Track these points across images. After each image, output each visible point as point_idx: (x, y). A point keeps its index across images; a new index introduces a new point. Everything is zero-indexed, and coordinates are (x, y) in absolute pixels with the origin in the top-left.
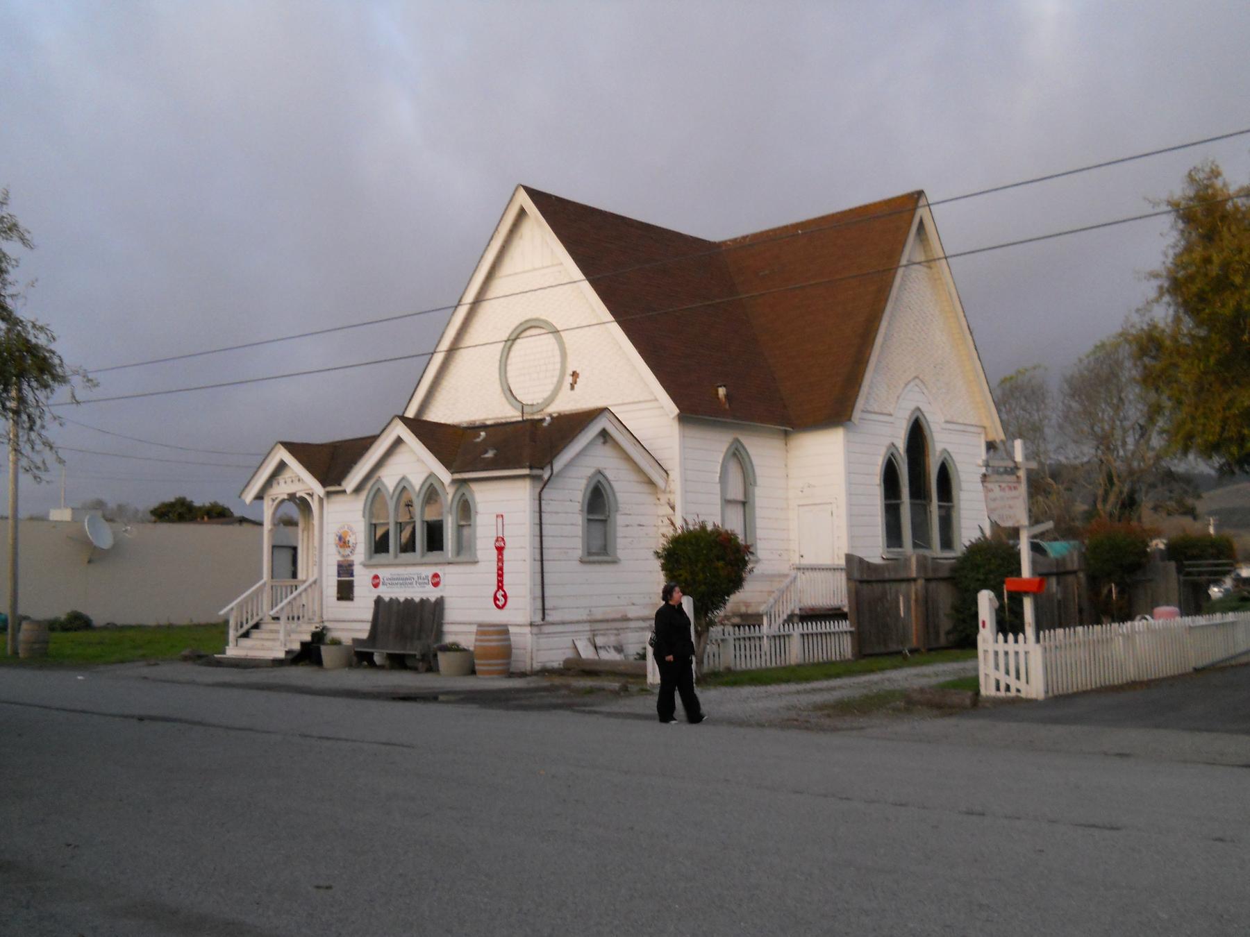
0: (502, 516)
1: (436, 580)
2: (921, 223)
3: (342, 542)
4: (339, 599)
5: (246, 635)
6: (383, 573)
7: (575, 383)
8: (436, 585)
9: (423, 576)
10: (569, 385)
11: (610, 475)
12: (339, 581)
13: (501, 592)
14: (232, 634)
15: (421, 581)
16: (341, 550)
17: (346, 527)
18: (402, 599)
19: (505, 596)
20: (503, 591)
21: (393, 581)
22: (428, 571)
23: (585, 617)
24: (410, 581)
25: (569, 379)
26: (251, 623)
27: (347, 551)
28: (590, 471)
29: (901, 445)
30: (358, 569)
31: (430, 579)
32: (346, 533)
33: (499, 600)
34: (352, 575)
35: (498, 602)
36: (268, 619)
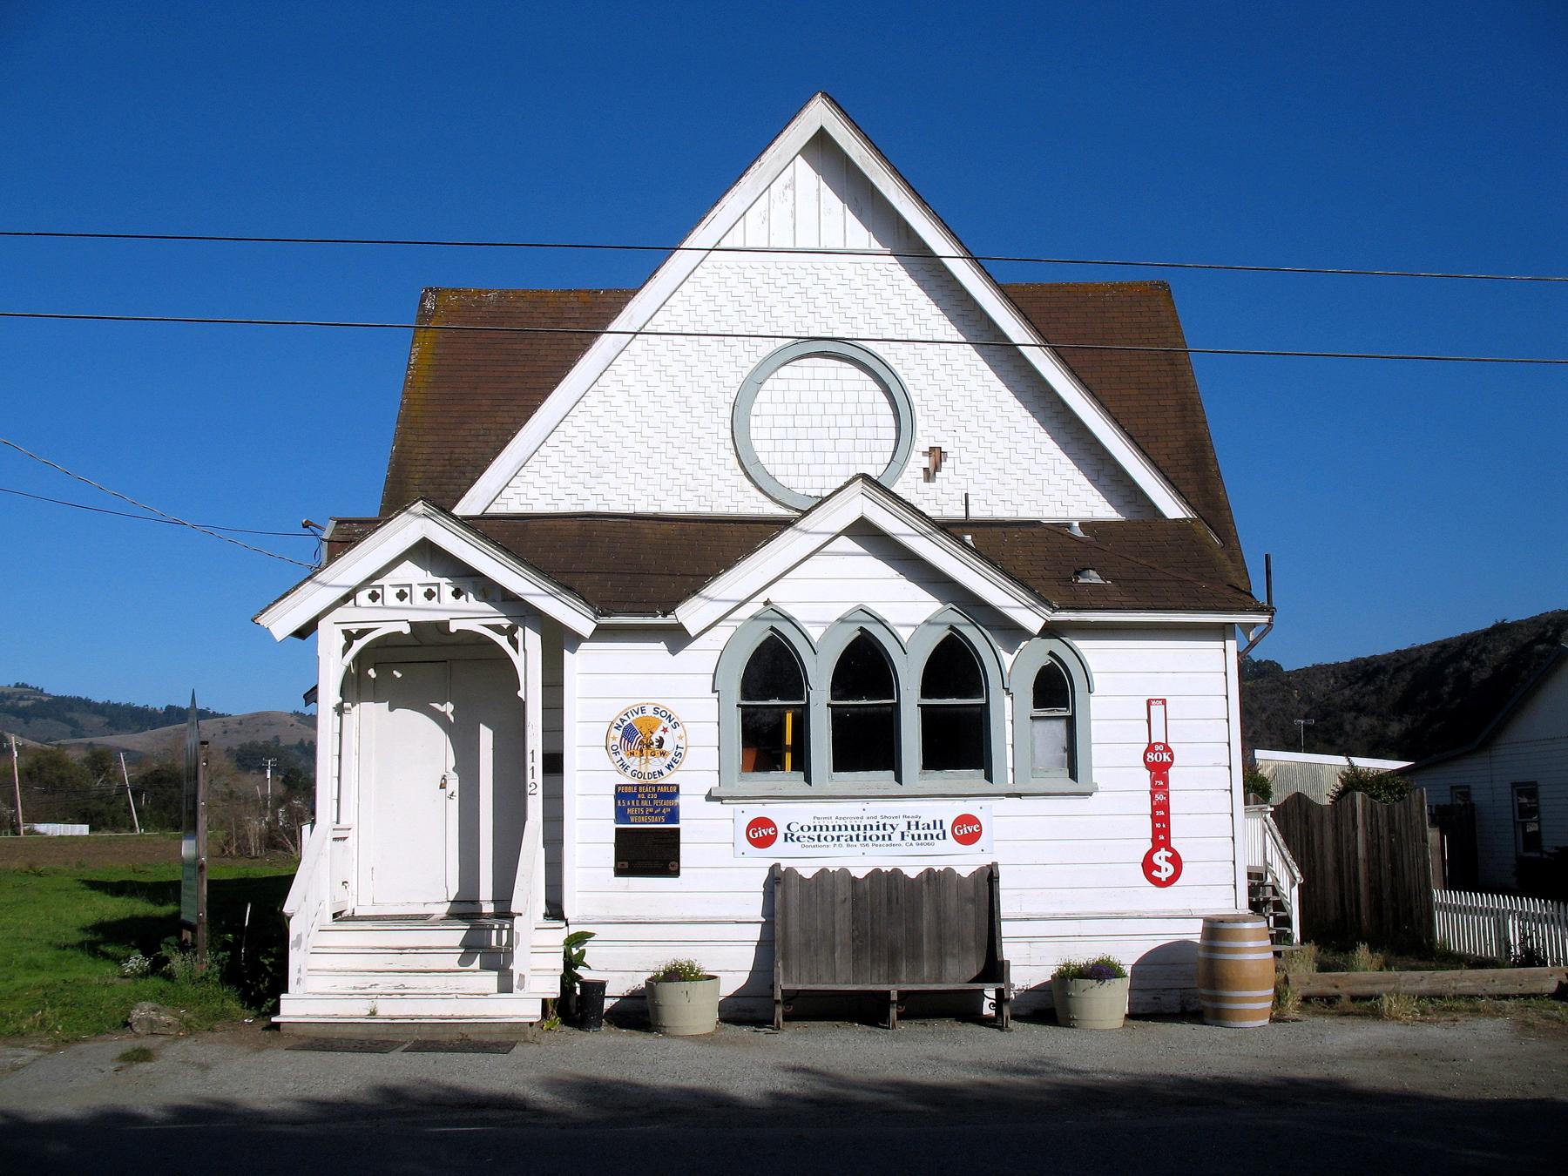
0: (1164, 702)
4: (619, 872)
6: (781, 814)
8: (969, 839)
10: (921, 474)
12: (617, 830)
13: (1163, 853)
15: (918, 832)
17: (649, 712)
19: (1176, 860)
20: (1169, 849)
21: (819, 833)
22: (949, 811)
24: (881, 833)
27: (656, 764)
34: (673, 816)
35: (1155, 873)
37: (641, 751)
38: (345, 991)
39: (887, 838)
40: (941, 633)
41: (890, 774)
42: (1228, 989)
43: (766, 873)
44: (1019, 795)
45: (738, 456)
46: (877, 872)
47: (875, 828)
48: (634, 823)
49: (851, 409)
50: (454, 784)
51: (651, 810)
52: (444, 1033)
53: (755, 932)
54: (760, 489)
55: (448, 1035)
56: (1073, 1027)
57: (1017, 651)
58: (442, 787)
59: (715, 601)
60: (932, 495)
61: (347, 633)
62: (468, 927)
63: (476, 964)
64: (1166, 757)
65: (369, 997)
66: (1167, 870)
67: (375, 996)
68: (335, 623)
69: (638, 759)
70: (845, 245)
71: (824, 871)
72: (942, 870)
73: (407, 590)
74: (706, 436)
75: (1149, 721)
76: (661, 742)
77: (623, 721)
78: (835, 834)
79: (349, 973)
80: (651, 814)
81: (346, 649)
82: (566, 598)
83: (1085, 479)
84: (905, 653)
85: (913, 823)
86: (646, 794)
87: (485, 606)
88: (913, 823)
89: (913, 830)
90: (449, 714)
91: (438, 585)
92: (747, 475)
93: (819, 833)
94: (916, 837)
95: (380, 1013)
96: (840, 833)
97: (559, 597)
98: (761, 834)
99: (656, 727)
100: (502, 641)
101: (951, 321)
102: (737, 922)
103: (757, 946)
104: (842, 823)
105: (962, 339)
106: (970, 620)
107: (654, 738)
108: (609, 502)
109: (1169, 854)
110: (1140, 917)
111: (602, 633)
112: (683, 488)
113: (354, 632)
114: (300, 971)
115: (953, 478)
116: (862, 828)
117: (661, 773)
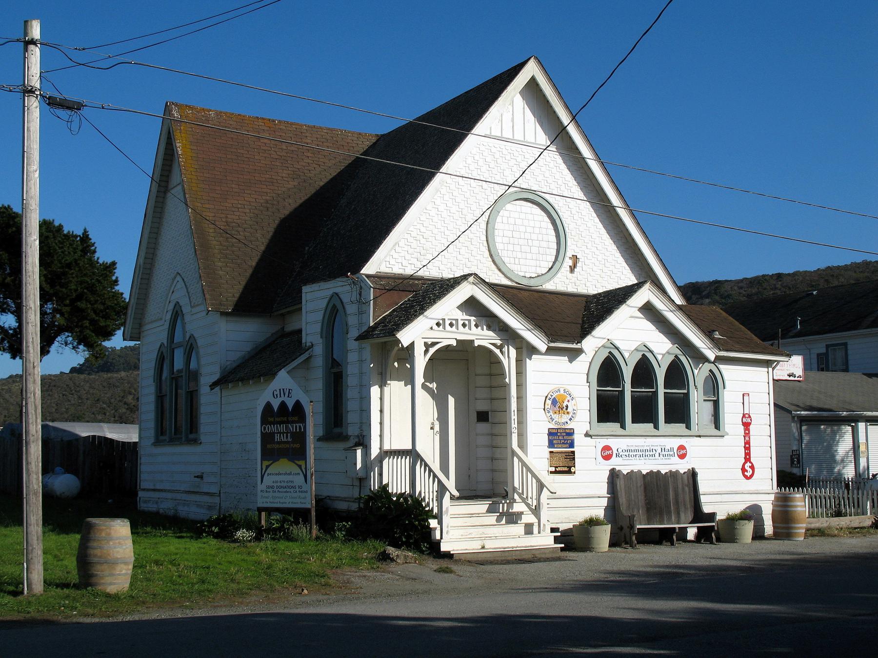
0: (749, 394)
1: (683, 452)
8: (682, 457)
9: (668, 447)
10: (568, 269)
13: (748, 464)
15: (665, 453)
17: (562, 392)
19: (752, 467)
20: (751, 462)
21: (629, 453)
22: (675, 443)
24: (651, 453)
25: (568, 262)
27: (565, 418)
31: (675, 451)
33: (747, 471)
34: (572, 445)
35: (746, 473)
37: (559, 411)
38: (458, 537)
39: (653, 455)
40: (672, 358)
41: (651, 425)
42: (795, 523)
43: (608, 473)
44: (700, 436)
45: (489, 250)
46: (651, 472)
47: (649, 451)
48: (556, 448)
49: (537, 230)
50: (437, 428)
51: (563, 441)
52: (525, 555)
53: (604, 502)
54: (500, 270)
55: (527, 556)
56: (737, 542)
57: (698, 368)
58: (432, 428)
59: (596, 338)
60: (574, 280)
61: (426, 344)
62: (491, 502)
63: (504, 522)
64: (749, 421)
65: (482, 539)
66: (748, 474)
67: (484, 538)
68: (423, 338)
69: (558, 415)
70: (536, 141)
71: (632, 471)
72: (663, 472)
73: (454, 322)
74: (474, 238)
75: (743, 403)
76: (567, 406)
77: (552, 396)
78: (635, 453)
79: (460, 528)
80: (563, 443)
81: (426, 352)
82: (537, 332)
83: (635, 278)
84: (627, 365)
85: (663, 449)
86: (561, 433)
87: (491, 333)
88: (663, 449)
89: (663, 453)
90: (434, 389)
91: (469, 321)
92: (494, 261)
93: (629, 453)
94: (664, 456)
95: (486, 547)
96: (636, 453)
97: (533, 332)
98: (607, 453)
99: (565, 399)
100: (497, 351)
101: (581, 189)
102: (599, 497)
103: (605, 509)
104: (637, 448)
105: (585, 199)
106: (682, 352)
107: (564, 405)
108: (430, 270)
109: (750, 465)
110: (743, 493)
111: (550, 351)
112: (464, 266)
113: (430, 343)
114: (448, 527)
115: (582, 272)
116: (644, 451)
117: (567, 423)
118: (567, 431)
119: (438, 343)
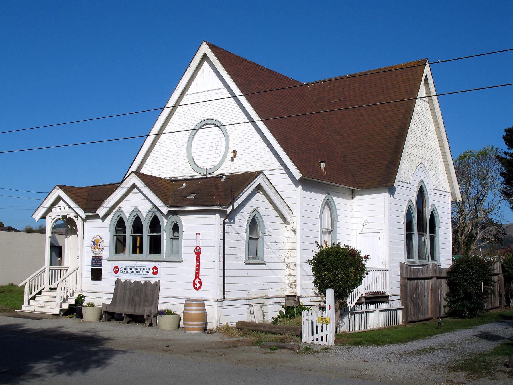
0: (200, 234)
1: (155, 271)
2: (426, 77)
3: (96, 244)
4: (92, 279)
5: (33, 298)
6: (121, 265)
7: (235, 157)
8: (155, 273)
9: (147, 268)
11: (261, 211)
12: (92, 268)
13: (198, 280)
14: (26, 298)
15: (145, 271)
16: (95, 250)
18: (132, 282)
19: (200, 282)
20: (199, 279)
21: (127, 270)
22: (151, 265)
23: (246, 296)
24: (138, 271)
26: (37, 291)
27: (99, 251)
28: (251, 210)
29: (414, 201)
30: (104, 262)
31: (151, 270)
32: (98, 240)
33: (196, 285)
34: (101, 265)
35: (195, 286)
36: (47, 289)
64: (200, 251)
76: (99, 245)
78: (129, 271)
80: (97, 264)
85: (144, 268)
86: (97, 259)
88: (144, 268)
89: (144, 271)
93: (127, 270)
95: (36, 311)
99: (99, 242)
104: (131, 268)
107: (98, 244)
109: (199, 281)
116: (135, 269)
117: (99, 254)
118: (99, 258)
119: (55, 218)
